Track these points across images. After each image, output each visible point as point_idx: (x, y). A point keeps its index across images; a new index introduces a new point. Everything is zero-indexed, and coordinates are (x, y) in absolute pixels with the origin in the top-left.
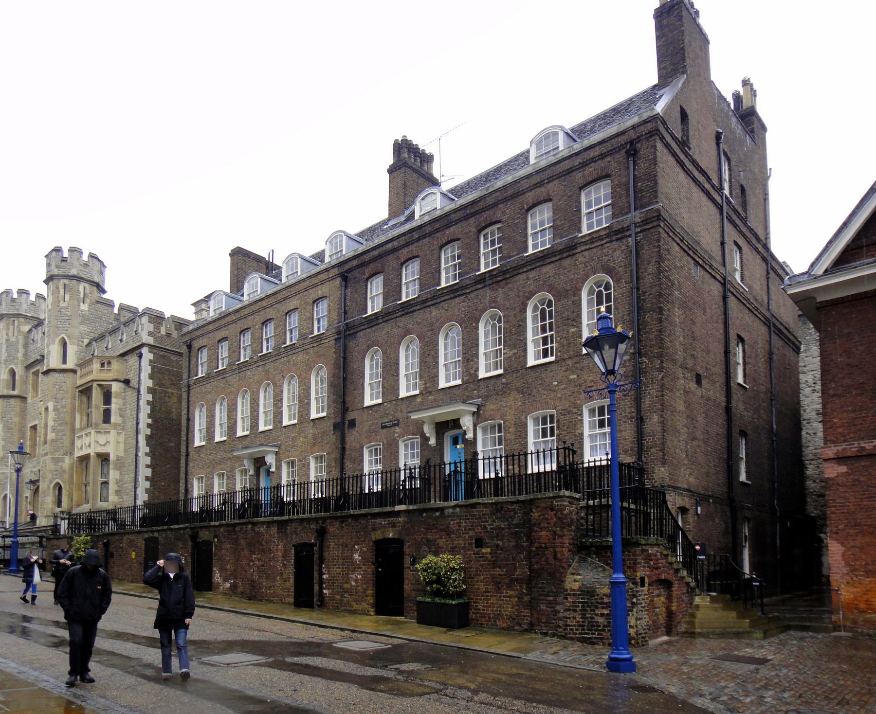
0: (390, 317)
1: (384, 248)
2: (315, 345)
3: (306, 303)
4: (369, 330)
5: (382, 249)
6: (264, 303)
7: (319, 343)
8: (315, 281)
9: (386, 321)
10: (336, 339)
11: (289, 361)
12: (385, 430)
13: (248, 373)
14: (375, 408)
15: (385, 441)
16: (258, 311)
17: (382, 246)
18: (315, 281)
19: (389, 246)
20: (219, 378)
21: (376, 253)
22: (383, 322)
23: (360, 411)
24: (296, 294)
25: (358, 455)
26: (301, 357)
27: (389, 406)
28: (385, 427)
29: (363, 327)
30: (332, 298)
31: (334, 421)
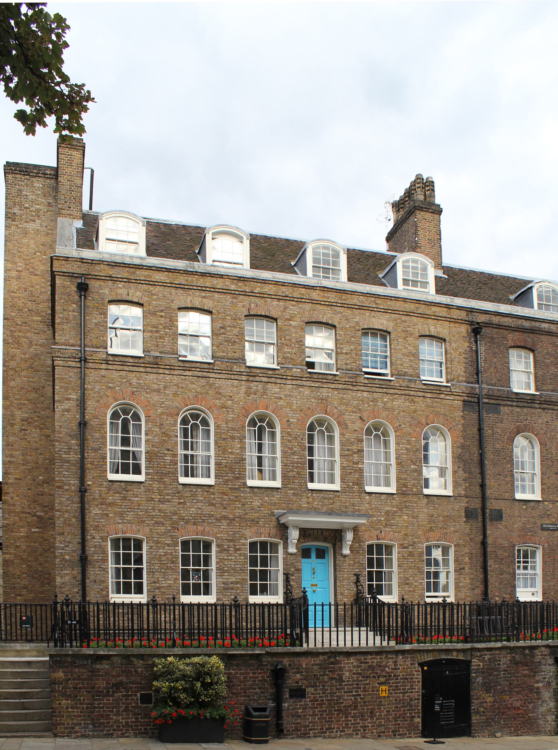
0: (551, 407)
1: (537, 324)
2: (429, 395)
3: (407, 334)
4: (518, 410)
5: (537, 324)
6: (315, 295)
7: (434, 396)
8: (423, 309)
9: (544, 409)
10: (464, 401)
11: (375, 400)
12: (546, 533)
13: (275, 389)
14: (532, 504)
15: (546, 545)
16: (300, 301)
17: (536, 321)
18: (423, 309)
19: (545, 326)
20: (188, 373)
21: (527, 324)
22: (540, 408)
23: (507, 502)
24: (386, 311)
25: (506, 554)
26: (399, 402)
27: (550, 506)
28: (548, 529)
29: (509, 403)
30: (454, 345)
31: (466, 505)
